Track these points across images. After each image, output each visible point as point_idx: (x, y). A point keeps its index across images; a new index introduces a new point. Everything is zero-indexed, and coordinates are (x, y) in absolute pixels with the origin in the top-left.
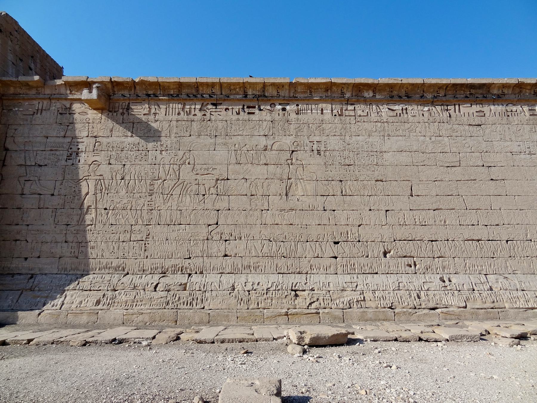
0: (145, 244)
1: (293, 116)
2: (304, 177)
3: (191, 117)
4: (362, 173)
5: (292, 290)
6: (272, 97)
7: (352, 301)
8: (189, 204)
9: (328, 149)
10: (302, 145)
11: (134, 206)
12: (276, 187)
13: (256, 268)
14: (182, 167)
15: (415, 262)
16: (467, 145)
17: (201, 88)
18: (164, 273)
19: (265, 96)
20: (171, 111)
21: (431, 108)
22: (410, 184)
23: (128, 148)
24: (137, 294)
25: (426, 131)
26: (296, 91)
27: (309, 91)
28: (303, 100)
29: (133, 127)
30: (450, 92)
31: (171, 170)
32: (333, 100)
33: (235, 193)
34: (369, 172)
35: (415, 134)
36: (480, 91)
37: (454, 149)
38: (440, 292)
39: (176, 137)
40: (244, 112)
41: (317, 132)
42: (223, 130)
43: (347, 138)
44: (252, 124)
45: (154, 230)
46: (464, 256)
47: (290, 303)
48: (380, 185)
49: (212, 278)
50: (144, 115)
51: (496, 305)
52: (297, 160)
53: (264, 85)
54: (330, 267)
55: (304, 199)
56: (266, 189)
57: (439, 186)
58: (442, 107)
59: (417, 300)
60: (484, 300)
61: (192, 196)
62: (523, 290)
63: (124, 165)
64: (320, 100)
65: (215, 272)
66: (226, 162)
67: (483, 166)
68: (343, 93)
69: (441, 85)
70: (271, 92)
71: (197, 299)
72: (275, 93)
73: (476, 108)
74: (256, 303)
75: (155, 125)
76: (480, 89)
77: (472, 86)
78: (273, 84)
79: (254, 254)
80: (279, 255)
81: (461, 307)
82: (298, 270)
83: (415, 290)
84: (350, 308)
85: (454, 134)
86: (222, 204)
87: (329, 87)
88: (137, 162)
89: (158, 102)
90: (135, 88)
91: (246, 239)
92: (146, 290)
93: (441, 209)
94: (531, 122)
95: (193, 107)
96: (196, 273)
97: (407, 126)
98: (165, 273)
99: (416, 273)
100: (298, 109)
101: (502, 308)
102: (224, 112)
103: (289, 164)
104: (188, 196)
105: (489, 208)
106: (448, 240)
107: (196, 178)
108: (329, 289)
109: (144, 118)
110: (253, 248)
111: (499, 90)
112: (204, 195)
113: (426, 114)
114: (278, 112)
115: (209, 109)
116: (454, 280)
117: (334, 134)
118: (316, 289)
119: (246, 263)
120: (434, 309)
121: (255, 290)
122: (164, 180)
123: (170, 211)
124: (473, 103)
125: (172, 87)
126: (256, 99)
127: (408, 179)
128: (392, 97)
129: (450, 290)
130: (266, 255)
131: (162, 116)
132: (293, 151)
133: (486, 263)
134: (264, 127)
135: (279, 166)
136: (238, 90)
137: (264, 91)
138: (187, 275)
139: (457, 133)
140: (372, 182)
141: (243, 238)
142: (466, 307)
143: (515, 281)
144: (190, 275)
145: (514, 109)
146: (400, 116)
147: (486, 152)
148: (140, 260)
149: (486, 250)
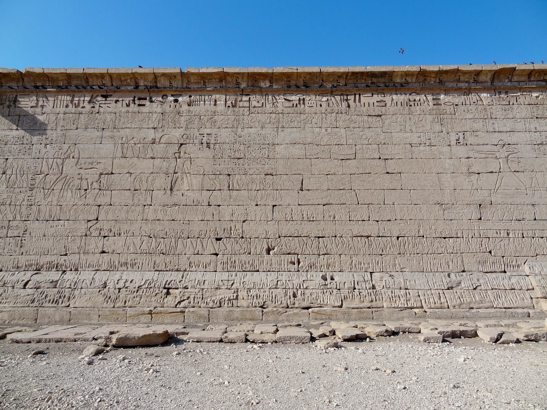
0: (22, 240)
1: (185, 107)
2: (191, 171)
3: (79, 109)
4: (251, 166)
5: (165, 288)
6: (164, 88)
7: (223, 299)
8: (70, 199)
9: (219, 142)
10: (192, 138)
11: (13, 201)
12: (162, 181)
13: (133, 266)
14: (66, 161)
15: (298, 259)
16: (364, 137)
17: (91, 80)
18: (38, 270)
19: (157, 87)
20: (59, 103)
21: (329, 98)
22: (301, 178)
23: (12, 141)
24: (5, 291)
25: (322, 122)
26: (189, 81)
27: (202, 82)
28: (195, 91)
29: (19, 120)
30: (350, 81)
31: (54, 164)
32: (226, 90)
33: (119, 188)
34: (259, 166)
35: (310, 126)
36: (382, 80)
37: (351, 141)
38: (318, 291)
39: (62, 130)
40: (135, 104)
41: (208, 125)
42: (111, 122)
43: (240, 130)
44: (141, 117)
45: (34, 227)
46: (351, 252)
47: (159, 301)
48: (269, 179)
49: (86, 275)
50: (32, 107)
51: (374, 304)
52: (185, 153)
53: (156, 76)
54: (210, 264)
55: (189, 193)
56: (150, 183)
57: (332, 180)
58: (342, 97)
59: (292, 298)
60: (362, 299)
61: (74, 191)
62: (406, 289)
63: (7, 159)
64: (214, 90)
65: (91, 269)
66: (111, 156)
67: (380, 158)
68: (238, 84)
69: (340, 74)
70: (163, 82)
71: (65, 297)
72: (167, 84)
73: (377, 98)
74: (124, 301)
75: (41, 118)
76: (381, 77)
77: (372, 75)
78: (164, 75)
79: (132, 251)
80: (158, 252)
81: (336, 307)
82: (177, 267)
83: (293, 288)
84: (220, 306)
85: (352, 125)
86: (104, 200)
87: (223, 77)
88: (21, 156)
89: (47, 94)
90: (23, 79)
91: (126, 235)
92: (15, 287)
93: (331, 204)
94: (434, 112)
95: (82, 99)
96: (71, 270)
97: (303, 117)
98: (39, 270)
99: (298, 271)
100: (190, 100)
101: (379, 308)
102: (113, 104)
103: (176, 158)
104: (69, 191)
105: (382, 203)
106: (336, 236)
107: (80, 172)
108: (203, 287)
109: (30, 111)
110: (132, 245)
111: (402, 79)
112: (86, 190)
113: (324, 105)
114: (170, 104)
115: (98, 101)
116: (336, 278)
117: (225, 126)
118: (189, 287)
119: (123, 260)
120: (307, 308)
121: (127, 288)
122: (47, 175)
123: (50, 207)
125: (61, 78)
126: (147, 90)
127: (299, 172)
128: (289, 87)
129: (330, 288)
130: (145, 251)
131: (50, 108)
132: (182, 144)
133: (374, 261)
134: (154, 119)
135: (166, 159)
136: (129, 81)
137: (156, 82)
138: (61, 272)
139: (355, 124)
140: (261, 176)
141: (122, 234)
142: (341, 306)
143: (399, 279)
144: (65, 271)
145: (417, 98)
146: (296, 106)
147: (384, 144)
148: (15, 257)
149: (375, 247)
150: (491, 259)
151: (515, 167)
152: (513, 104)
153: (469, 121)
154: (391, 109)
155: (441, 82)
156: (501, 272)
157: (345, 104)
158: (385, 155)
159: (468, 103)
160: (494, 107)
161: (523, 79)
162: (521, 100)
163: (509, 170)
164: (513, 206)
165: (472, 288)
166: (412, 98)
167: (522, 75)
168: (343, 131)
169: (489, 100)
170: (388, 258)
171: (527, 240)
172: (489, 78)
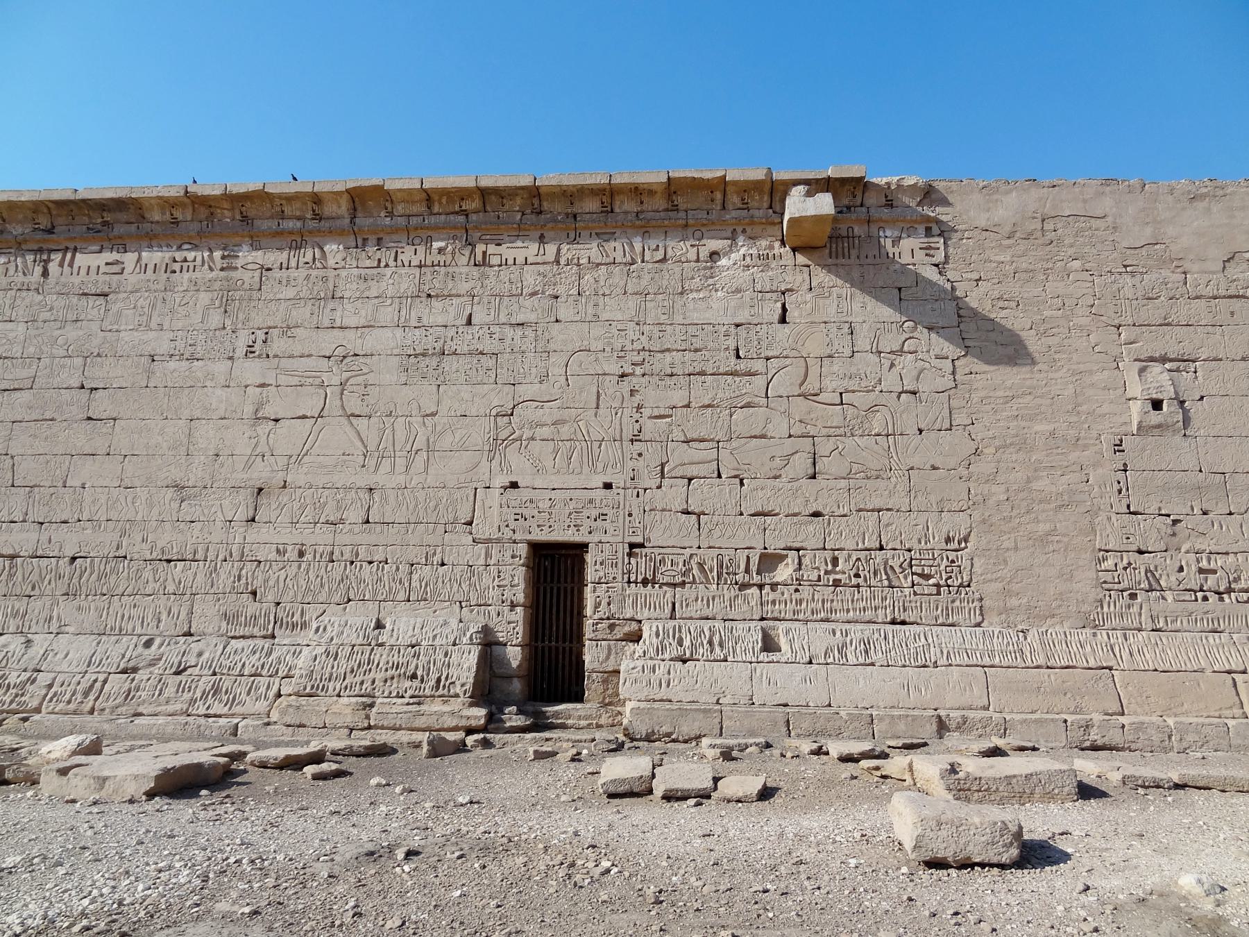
16: (60, 341)
37: (32, 349)
67: (83, 387)
76: (121, 211)
85: (45, 315)
94: (217, 285)
105: (60, 484)
111: (164, 214)
124: (106, 244)
145: (190, 255)
147: (99, 355)
149: (20, 578)
150: (252, 608)
151: (354, 405)
152: (387, 266)
153: (284, 305)
154: (132, 278)
155: (245, 218)
156: (264, 637)
157: (38, 270)
158: (93, 379)
159: (293, 263)
160: (344, 273)
161: (416, 209)
162: (407, 254)
163: (341, 412)
164: (327, 492)
165: (174, 669)
166: (179, 256)
167: (413, 202)
168: (21, 328)
169: (339, 257)
170: (39, 603)
171: (337, 570)
172: (344, 208)
